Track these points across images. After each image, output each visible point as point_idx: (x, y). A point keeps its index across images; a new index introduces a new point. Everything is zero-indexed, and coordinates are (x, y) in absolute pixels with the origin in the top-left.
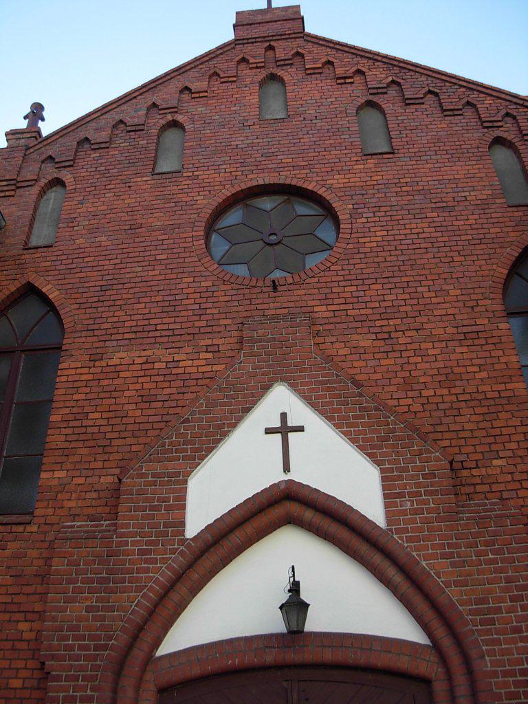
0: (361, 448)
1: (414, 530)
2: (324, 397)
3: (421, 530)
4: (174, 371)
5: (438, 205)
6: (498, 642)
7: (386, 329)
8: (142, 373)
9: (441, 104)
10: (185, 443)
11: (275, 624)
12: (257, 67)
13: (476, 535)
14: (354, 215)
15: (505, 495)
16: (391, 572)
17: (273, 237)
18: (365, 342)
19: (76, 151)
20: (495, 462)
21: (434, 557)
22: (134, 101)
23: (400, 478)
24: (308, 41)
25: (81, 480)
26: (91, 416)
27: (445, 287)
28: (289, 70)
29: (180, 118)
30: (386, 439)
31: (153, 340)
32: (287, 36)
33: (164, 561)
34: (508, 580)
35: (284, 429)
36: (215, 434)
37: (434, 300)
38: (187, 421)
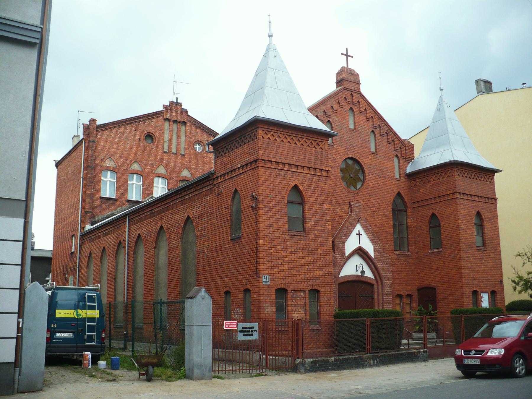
0: (371, 241)
3: (378, 259)
4: (338, 214)
9: (388, 138)
13: (385, 261)
15: (388, 253)
17: (351, 175)
20: (387, 246)
23: (376, 248)
29: (331, 120)
30: (374, 239)
32: (356, 92)
33: (343, 261)
35: (359, 234)
36: (348, 234)
37: (381, 205)
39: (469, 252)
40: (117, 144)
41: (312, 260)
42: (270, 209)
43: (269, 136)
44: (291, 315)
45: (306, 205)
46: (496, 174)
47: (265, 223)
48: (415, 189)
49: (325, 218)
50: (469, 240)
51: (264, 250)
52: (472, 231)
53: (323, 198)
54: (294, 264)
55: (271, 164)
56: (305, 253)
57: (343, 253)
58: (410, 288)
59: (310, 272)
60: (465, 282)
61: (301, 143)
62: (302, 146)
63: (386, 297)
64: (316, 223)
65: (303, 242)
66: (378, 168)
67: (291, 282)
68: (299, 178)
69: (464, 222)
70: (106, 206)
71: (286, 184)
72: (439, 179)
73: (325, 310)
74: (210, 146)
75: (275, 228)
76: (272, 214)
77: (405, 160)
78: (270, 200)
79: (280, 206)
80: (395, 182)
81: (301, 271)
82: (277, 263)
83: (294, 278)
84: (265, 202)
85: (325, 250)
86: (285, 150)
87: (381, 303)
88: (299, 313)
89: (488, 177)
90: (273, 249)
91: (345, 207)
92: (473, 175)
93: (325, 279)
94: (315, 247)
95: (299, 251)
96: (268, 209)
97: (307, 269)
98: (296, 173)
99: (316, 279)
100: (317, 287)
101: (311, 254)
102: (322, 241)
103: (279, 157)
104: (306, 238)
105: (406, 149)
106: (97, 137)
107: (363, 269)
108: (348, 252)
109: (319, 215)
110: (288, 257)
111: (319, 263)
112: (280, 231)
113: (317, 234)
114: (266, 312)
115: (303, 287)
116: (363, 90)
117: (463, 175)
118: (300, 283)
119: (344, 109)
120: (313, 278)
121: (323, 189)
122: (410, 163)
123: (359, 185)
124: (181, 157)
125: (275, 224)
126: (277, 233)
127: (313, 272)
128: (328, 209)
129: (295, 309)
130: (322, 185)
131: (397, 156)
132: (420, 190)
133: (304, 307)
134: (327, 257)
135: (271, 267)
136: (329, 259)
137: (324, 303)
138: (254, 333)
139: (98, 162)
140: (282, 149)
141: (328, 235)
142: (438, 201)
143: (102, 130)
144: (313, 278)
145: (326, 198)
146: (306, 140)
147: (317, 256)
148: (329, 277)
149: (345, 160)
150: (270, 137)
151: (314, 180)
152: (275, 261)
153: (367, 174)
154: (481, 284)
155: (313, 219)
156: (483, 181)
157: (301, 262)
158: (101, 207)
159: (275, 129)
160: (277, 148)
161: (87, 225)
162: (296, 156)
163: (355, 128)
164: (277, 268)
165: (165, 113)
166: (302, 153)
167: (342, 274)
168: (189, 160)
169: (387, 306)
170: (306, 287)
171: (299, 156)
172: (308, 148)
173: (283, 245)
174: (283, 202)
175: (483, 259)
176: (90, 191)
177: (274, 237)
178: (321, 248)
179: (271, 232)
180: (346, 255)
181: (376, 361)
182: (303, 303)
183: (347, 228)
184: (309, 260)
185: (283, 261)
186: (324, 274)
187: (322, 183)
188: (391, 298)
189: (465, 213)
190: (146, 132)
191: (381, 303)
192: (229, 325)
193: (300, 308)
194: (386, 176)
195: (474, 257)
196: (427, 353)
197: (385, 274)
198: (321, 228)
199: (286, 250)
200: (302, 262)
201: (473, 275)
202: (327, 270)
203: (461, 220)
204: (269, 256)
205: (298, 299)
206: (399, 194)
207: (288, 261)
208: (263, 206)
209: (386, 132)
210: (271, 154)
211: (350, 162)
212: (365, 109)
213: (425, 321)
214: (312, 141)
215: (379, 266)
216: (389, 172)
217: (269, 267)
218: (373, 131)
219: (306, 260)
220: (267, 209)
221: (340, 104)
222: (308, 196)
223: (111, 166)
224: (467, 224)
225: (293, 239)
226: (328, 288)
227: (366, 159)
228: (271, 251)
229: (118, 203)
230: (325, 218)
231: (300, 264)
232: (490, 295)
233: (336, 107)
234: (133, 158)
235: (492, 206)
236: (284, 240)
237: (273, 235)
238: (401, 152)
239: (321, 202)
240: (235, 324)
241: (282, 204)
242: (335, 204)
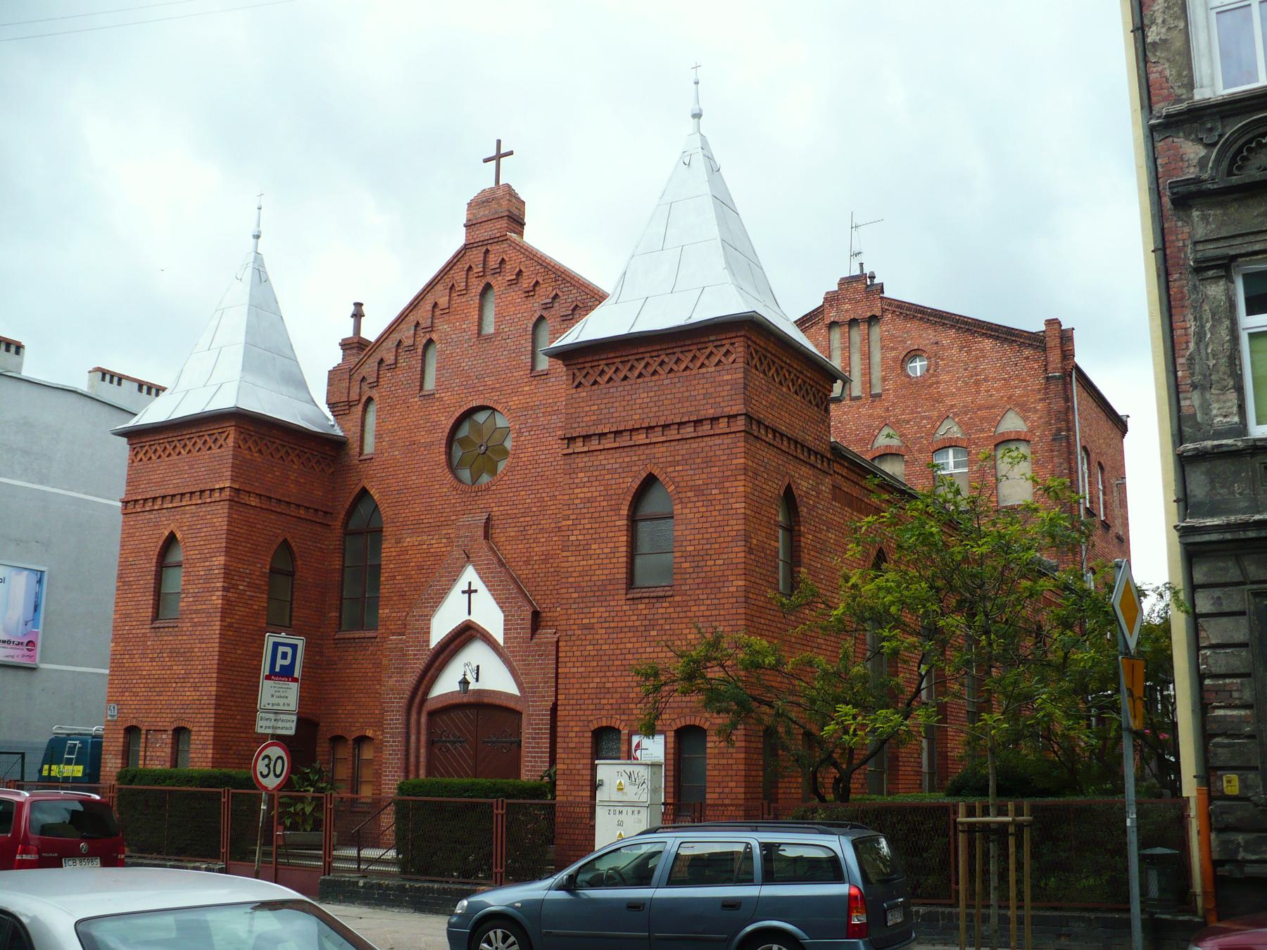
0: (498, 603)
11: (457, 688)
12: (479, 277)
13: (536, 651)
17: (482, 448)
19: (378, 371)
21: (519, 660)
22: (406, 319)
23: (511, 620)
25: (395, 614)
26: (397, 578)
30: (508, 598)
31: (421, 530)
35: (470, 592)
37: (549, 503)
41: (183, 672)
49: (212, 585)
52: (611, 545)
53: (213, 546)
57: (424, 642)
60: (566, 702)
65: (171, 638)
68: (178, 517)
91: (450, 531)
95: (165, 655)
99: (185, 707)
101: (181, 659)
113: (196, 620)
119: (467, 296)
123: (502, 466)
124: (872, 402)
154: (632, 706)
155: (191, 591)
168: (894, 404)
169: (532, 766)
178: (199, 645)
183: (439, 581)
195: (612, 625)
201: (604, 680)
213: (225, 800)
224: (594, 526)
225: (159, 634)
230: (212, 585)
232: (671, 740)
235: (717, 442)
242: (426, 530)
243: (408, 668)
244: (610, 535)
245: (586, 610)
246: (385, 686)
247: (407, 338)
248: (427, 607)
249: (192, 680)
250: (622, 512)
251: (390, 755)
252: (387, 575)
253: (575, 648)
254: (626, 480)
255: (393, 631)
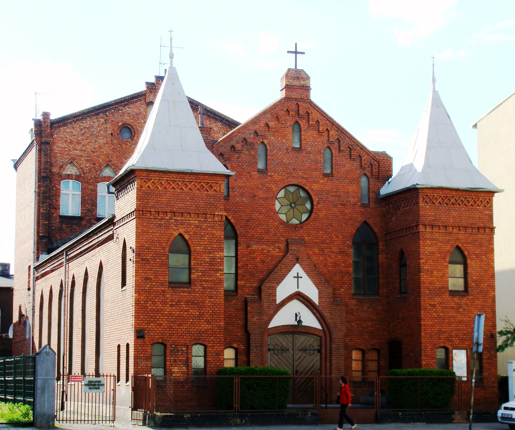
1: (324, 306)
2: (307, 269)
3: (325, 306)
4: (271, 254)
5: (342, 203)
6: (336, 332)
7: (322, 247)
8: (261, 253)
10: (276, 279)
14: (318, 203)
16: (317, 314)
17: (293, 205)
18: (316, 251)
20: (342, 290)
23: (322, 293)
24: (312, 106)
26: (249, 265)
27: (339, 235)
28: (303, 121)
29: (266, 141)
30: (320, 283)
34: (341, 319)
35: (298, 277)
36: (282, 277)
37: (335, 239)
38: (276, 272)
39: (435, 298)
40: (80, 143)
42: (148, 262)
43: (149, 184)
44: (169, 370)
45: (192, 254)
46: (495, 194)
47: (142, 276)
48: (388, 216)
49: (216, 267)
50: (438, 283)
51: (139, 305)
53: (215, 246)
54: (175, 318)
55: (150, 215)
56: (189, 306)
57: (272, 300)
58: (376, 341)
59: (195, 325)
61: (188, 187)
62: (190, 191)
63: (334, 351)
64: (204, 274)
65: (186, 294)
66: (334, 194)
67: (170, 337)
68: (185, 226)
69: (431, 261)
70: (68, 227)
71: (168, 235)
72: (407, 206)
73: (213, 366)
74: (111, 187)
75: (153, 281)
76: (149, 267)
77: (378, 179)
78: (148, 253)
79: (159, 258)
80: (360, 210)
81: (183, 325)
82: (154, 317)
83: (174, 332)
84: (142, 255)
85: (214, 302)
86: (168, 197)
87: (328, 358)
88: (180, 368)
89: (480, 200)
90: (151, 303)
92: (453, 200)
93: (213, 333)
94: (201, 299)
95: (181, 303)
96: (145, 262)
97: (190, 323)
98: (181, 221)
99: (202, 333)
100: (203, 341)
101: (196, 306)
102: (211, 293)
103: (161, 206)
104: (190, 290)
105: (379, 166)
106: (52, 135)
107: (300, 318)
108: (279, 299)
109: (208, 265)
110: (167, 310)
111: (206, 316)
112: (158, 284)
113: (206, 286)
114: (140, 367)
115: (185, 342)
116: (315, 97)
117: (434, 202)
118: (181, 337)
120: (198, 333)
121: (214, 236)
122: (387, 183)
125: (153, 277)
126: (155, 286)
127: (198, 325)
128: (220, 258)
129: (176, 364)
130: (214, 232)
131: (365, 174)
132: (393, 219)
133: (186, 363)
134: (217, 309)
135: (147, 322)
136: (219, 312)
137: (211, 359)
138: (101, 387)
139: (55, 170)
140: (164, 197)
141: (220, 286)
142: (405, 234)
143: (59, 127)
144: (198, 333)
145: (219, 246)
146: (196, 184)
147: (204, 309)
148: (219, 330)
149: (284, 187)
150: (150, 186)
151: (203, 227)
152: (153, 315)
153: (315, 203)
154: (453, 339)
155: (201, 269)
156: (472, 205)
157: (183, 315)
158: (61, 229)
159: (156, 176)
160: (158, 197)
161: (42, 254)
162: (182, 203)
163: (301, 147)
164: (155, 322)
165: (147, 95)
166: (189, 198)
167: (272, 324)
170: (189, 342)
171: (185, 203)
172: (198, 192)
173: (162, 298)
174: (164, 253)
175: (458, 308)
176: (44, 210)
177: (151, 291)
178: (210, 300)
179: (148, 286)
180: (278, 301)
181: (244, 421)
182: (185, 359)
183: (281, 271)
184: (194, 313)
185: (161, 315)
186: (212, 328)
187: (214, 229)
188: (342, 354)
189: (432, 250)
190: (120, 124)
191: (328, 358)
192: (74, 379)
193: (181, 363)
194: (346, 203)
195: (444, 305)
196: (316, 415)
197: (335, 323)
198: (211, 279)
199: (165, 303)
200: (185, 315)
201: (441, 328)
202: (217, 323)
203: (426, 259)
204: (145, 310)
205: (179, 354)
206: (365, 222)
207: (167, 315)
208: (140, 260)
209: (349, 147)
210: (151, 203)
211: (292, 189)
212: (317, 120)
214: (204, 184)
215: (326, 314)
216: (351, 197)
217: (145, 322)
218: (328, 147)
219: (190, 313)
220: (144, 262)
221: (279, 119)
222: (195, 245)
223: (74, 173)
226: (217, 342)
227: (315, 185)
228: (147, 305)
229: (84, 222)
230: (216, 267)
231: (183, 318)
233: (271, 124)
234: (103, 160)
236: (163, 293)
237: (150, 288)
238: (372, 169)
239: (212, 251)
240: (81, 378)
241: (162, 256)
242: (266, 243)
243: (264, 313)
244: (441, 268)
245: (433, 299)
246: (250, 321)
247: (251, 138)
248: (274, 283)
249: (205, 318)
250: (446, 260)
251: (255, 357)
252: (242, 263)
253: (428, 314)
254: (448, 247)
255: (248, 293)
